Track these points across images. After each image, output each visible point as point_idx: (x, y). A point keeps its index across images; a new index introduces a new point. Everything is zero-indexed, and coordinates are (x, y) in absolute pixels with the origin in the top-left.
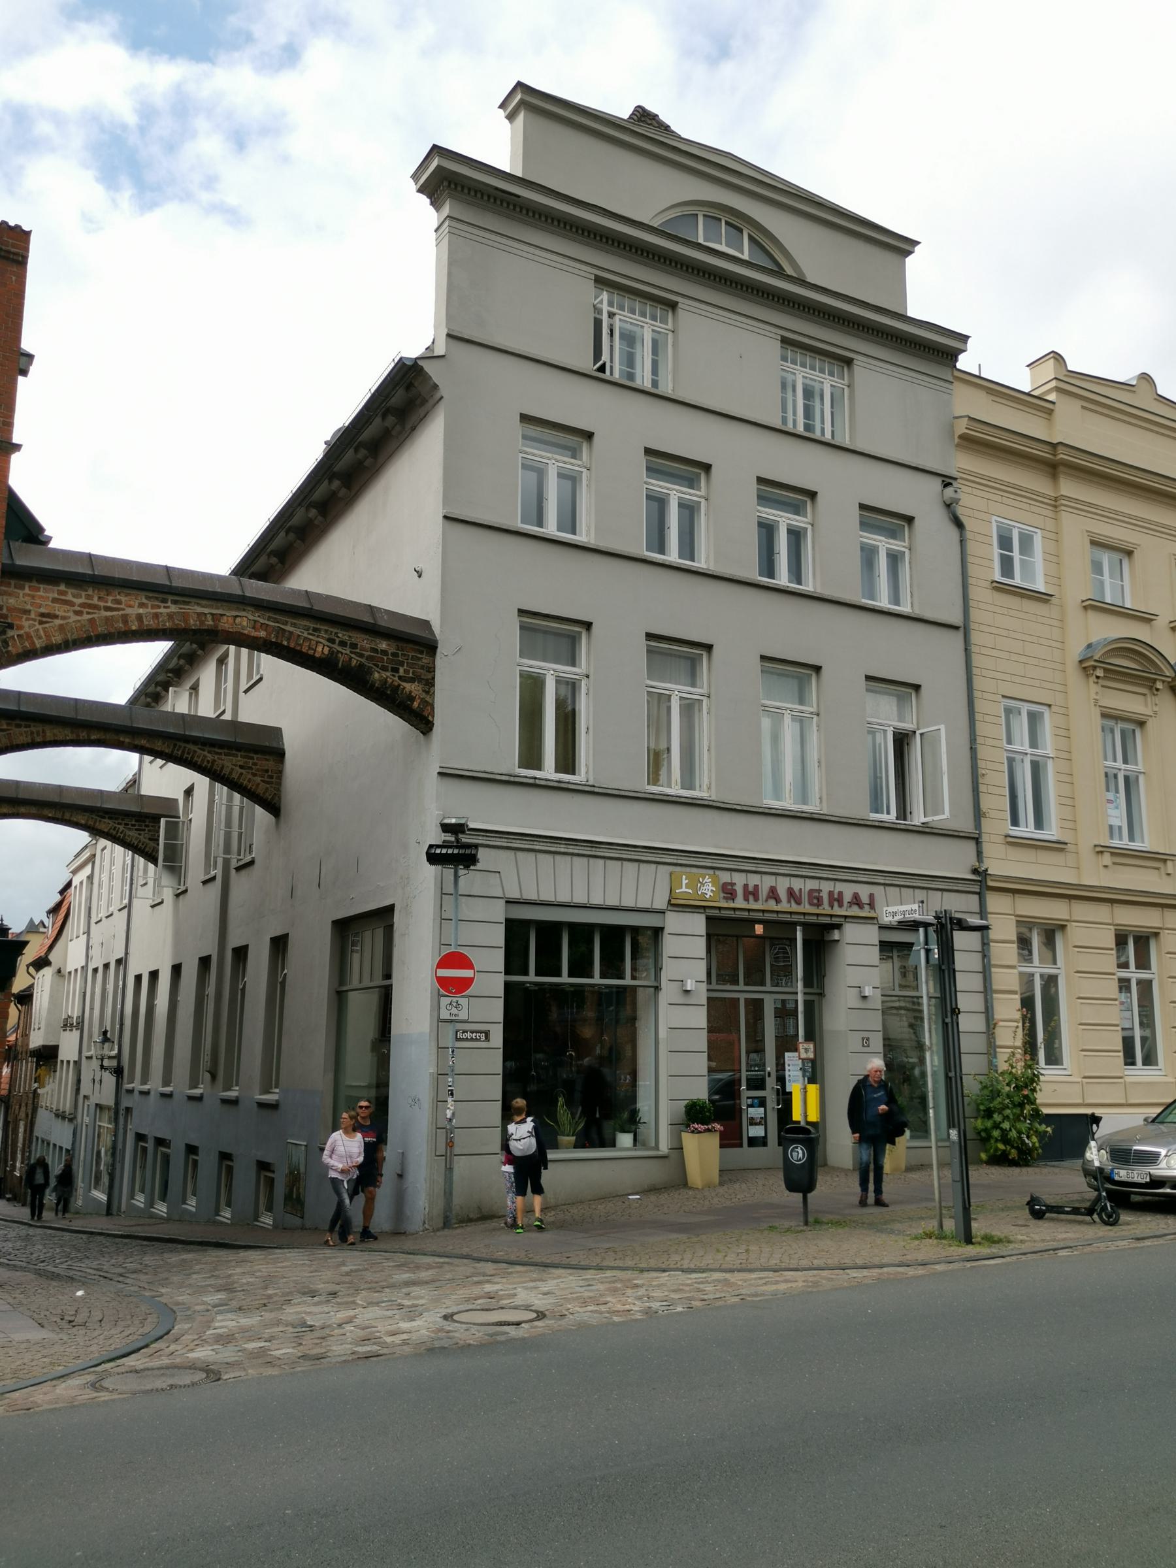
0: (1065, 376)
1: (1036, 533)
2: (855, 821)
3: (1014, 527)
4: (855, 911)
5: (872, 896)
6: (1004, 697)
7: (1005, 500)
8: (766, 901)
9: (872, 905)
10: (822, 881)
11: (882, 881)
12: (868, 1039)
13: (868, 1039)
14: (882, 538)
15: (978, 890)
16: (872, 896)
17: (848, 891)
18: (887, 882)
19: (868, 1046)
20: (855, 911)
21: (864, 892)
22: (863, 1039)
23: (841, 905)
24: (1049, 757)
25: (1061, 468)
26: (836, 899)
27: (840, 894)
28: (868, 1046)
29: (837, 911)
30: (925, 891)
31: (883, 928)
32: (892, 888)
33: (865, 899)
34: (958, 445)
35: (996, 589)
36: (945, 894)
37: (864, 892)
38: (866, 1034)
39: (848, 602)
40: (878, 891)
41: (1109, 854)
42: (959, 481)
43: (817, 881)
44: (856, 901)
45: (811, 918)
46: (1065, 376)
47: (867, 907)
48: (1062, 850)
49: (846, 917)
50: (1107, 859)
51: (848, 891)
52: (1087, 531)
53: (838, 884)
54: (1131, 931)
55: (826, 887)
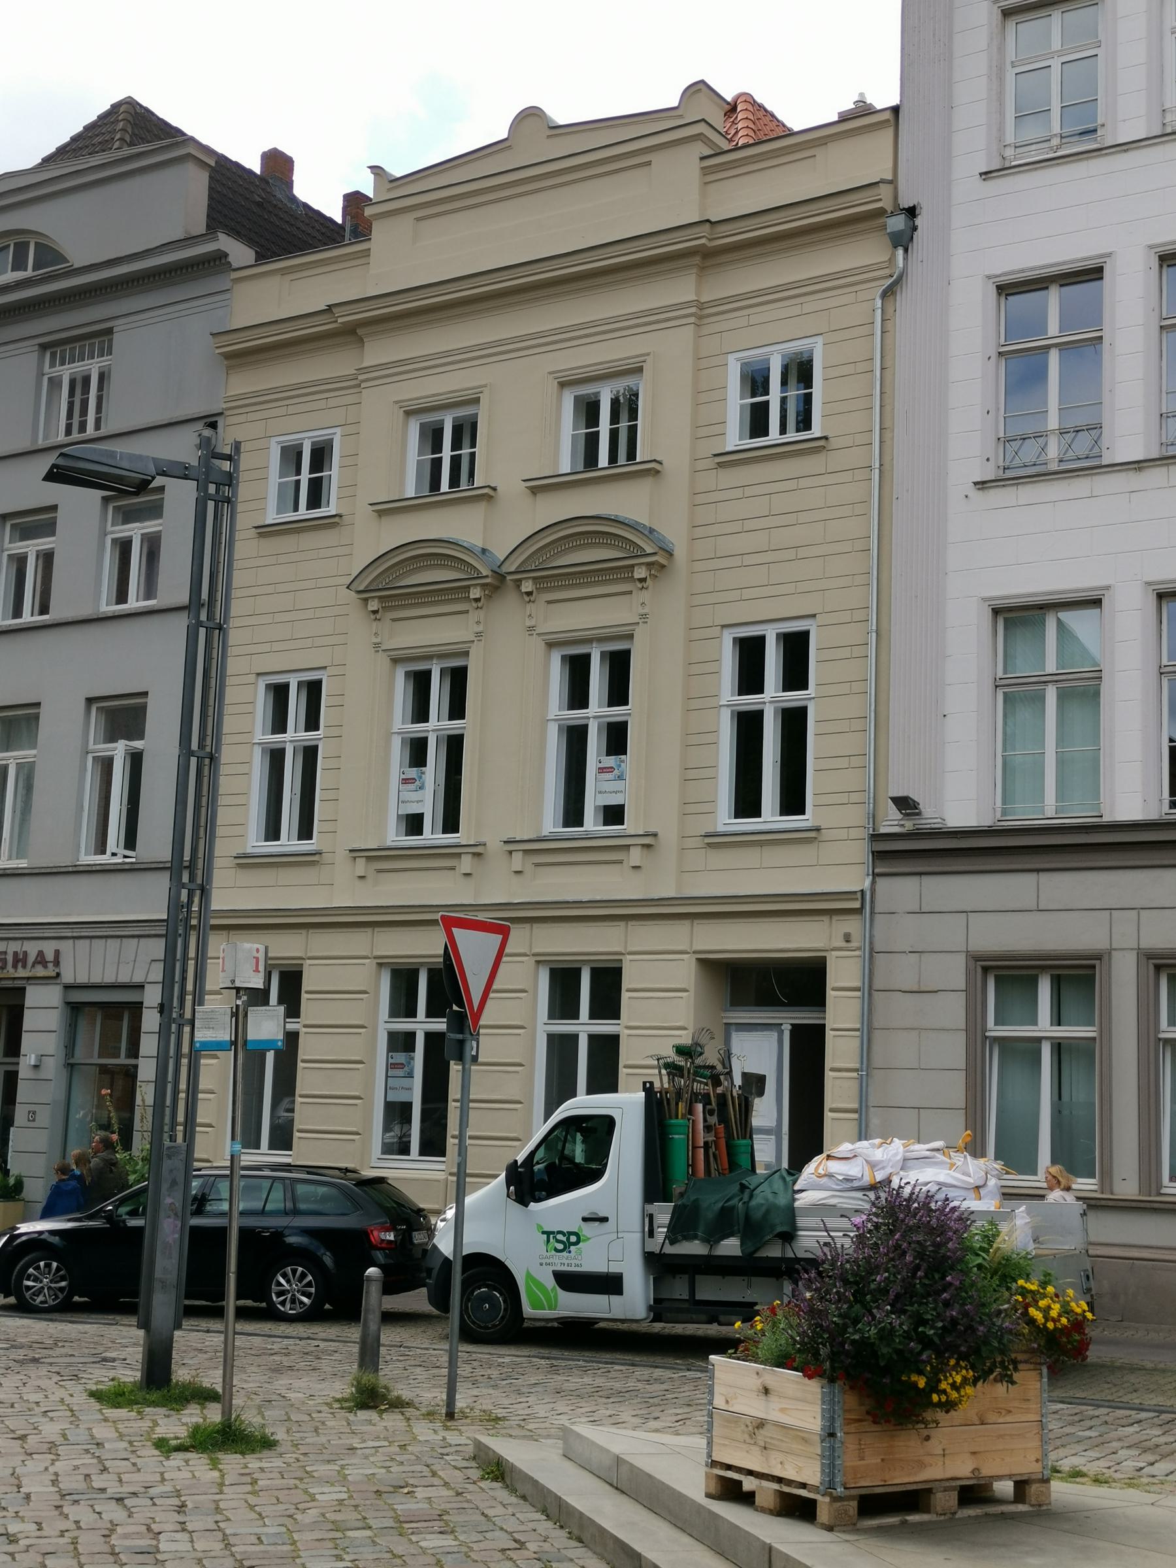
0: (389, 190)
1: (335, 434)
2: (48, 870)
3: (304, 439)
4: (40, 971)
5: (57, 953)
6: (258, 674)
7: (291, 410)
8: (33, 966)
9: (57, 963)
10: (10, 942)
11: (70, 934)
12: (34, 1113)
13: (34, 1113)
14: (137, 524)
15: (164, 932)
16: (57, 953)
17: (32, 948)
18: (75, 934)
19: (34, 1120)
20: (40, 971)
21: (49, 948)
22: (29, 1112)
23: (24, 966)
24: (320, 739)
25: (360, 332)
26: (20, 960)
27: (25, 953)
28: (34, 1120)
29: (21, 973)
30: (119, 940)
31: (67, 987)
32: (82, 941)
33: (50, 956)
34: (229, 368)
35: (261, 535)
36: (143, 941)
37: (49, 948)
38: (32, 1108)
39: (70, 620)
40: (65, 947)
41: (364, 859)
42: (227, 413)
43: (20, 942)
44: (41, 960)
45: (19, 982)
46: (389, 190)
47: (50, 965)
48: (313, 863)
49: (28, 978)
50: (361, 867)
51: (32, 948)
52: (396, 402)
53: (25, 942)
54: (422, 964)
55: (14, 947)
